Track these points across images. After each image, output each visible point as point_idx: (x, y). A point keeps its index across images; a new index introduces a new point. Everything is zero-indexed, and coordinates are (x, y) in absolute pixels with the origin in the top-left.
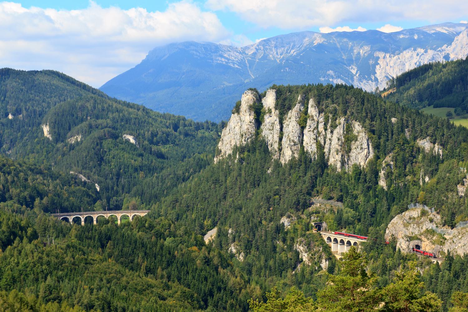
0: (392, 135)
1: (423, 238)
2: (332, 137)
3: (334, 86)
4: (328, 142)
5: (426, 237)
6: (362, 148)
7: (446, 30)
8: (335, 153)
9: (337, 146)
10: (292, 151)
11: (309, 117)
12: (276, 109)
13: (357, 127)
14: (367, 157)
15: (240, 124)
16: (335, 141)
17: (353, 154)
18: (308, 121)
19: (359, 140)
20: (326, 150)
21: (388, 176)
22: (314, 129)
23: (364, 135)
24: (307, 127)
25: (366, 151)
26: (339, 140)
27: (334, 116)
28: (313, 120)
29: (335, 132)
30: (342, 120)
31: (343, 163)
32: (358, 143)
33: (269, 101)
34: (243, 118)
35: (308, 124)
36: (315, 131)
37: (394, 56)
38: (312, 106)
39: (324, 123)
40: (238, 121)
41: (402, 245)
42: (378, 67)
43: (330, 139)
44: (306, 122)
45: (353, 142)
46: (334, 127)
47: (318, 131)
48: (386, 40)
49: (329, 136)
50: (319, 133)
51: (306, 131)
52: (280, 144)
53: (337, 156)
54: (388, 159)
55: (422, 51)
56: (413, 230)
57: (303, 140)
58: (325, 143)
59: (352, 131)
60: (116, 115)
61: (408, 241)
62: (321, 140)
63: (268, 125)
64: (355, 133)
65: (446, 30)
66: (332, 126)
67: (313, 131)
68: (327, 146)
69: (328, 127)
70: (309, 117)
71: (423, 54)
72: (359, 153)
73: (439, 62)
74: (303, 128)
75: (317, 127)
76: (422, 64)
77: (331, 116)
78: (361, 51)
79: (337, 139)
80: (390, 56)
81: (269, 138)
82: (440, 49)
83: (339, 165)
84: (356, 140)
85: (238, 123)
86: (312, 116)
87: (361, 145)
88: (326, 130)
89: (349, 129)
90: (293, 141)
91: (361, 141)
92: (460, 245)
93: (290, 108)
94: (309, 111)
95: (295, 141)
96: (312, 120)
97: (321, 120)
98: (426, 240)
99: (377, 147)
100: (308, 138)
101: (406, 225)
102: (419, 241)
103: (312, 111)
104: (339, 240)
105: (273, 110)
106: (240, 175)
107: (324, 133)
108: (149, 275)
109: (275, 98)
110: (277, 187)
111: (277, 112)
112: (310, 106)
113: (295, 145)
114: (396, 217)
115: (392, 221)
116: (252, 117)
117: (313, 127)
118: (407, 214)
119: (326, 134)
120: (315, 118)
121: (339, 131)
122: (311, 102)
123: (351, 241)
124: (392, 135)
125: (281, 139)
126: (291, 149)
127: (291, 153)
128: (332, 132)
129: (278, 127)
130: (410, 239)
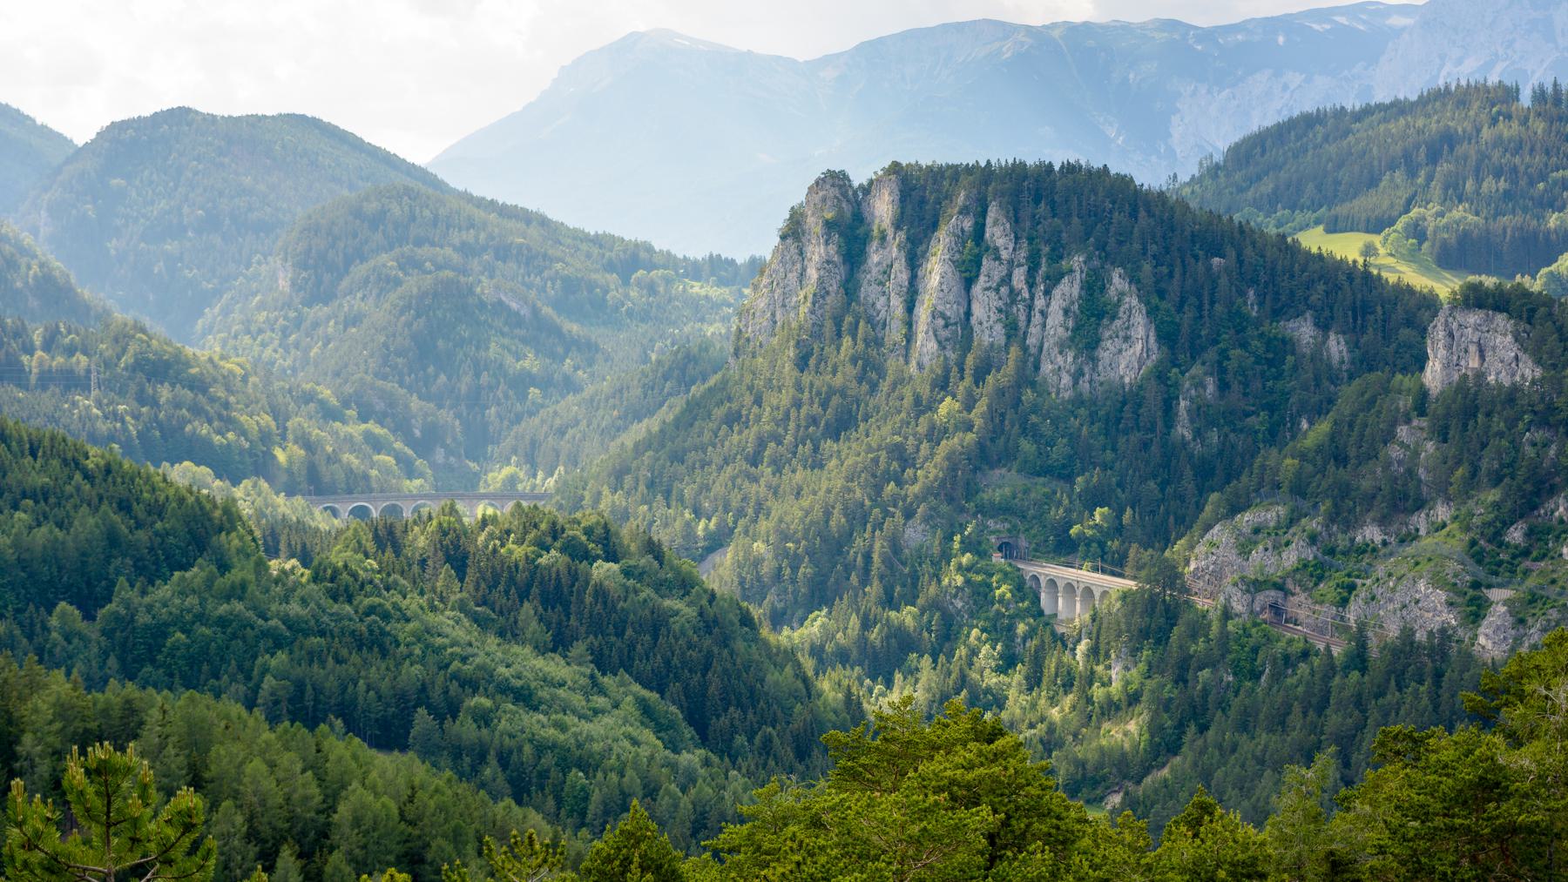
0: (1212, 303)
1: (1290, 585)
2: (1048, 305)
3: (1057, 168)
4: (1037, 319)
5: (1300, 583)
6: (1127, 339)
7: (1364, 22)
8: (1056, 350)
9: (1061, 330)
10: (939, 342)
11: (987, 249)
12: (897, 227)
13: (1117, 281)
14: (1141, 362)
15: (799, 266)
16: (1056, 317)
17: (1105, 354)
18: (985, 262)
19: (1121, 314)
20: (1031, 341)
21: (1200, 412)
22: (999, 285)
23: (1135, 302)
24: (982, 279)
25: (1139, 346)
26: (1066, 312)
27: (1053, 250)
28: (998, 258)
29: (1057, 292)
30: (1077, 261)
31: (1077, 375)
32: (1118, 323)
33: (883, 209)
34: (809, 249)
35: (983, 269)
36: (1004, 290)
37: (1219, 92)
38: (996, 223)
39: (1026, 267)
40: (796, 257)
41: (1234, 604)
42: (1175, 119)
43: (1042, 312)
44: (979, 265)
45: (1105, 321)
46: (1054, 280)
47: (1012, 290)
48: (1199, 47)
49: (1039, 303)
50: (1013, 293)
51: (977, 289)
52: (909, 324)
53: (1060, 359)
54: (1196, 370)
55: (1295, 79)
56: (1260, 560)
57: (968, 314)
58: (1029, 321)
59: (1103, 289)
60: (469, 236)
61: (1248, 591)
62: (1020, 311)
63: (875, 270)
64: (1112, 292)
65: (1364, 22)
66: (1048, 277)
67: (997, 290)
68: (1033, 330)
69: (1039, 279)
70: (987, 249)
71: (1300, 86)
72: (1120, 351)
73: (1343, 108)
74: (969, 283)
75: (1007, 280)
76: (1296, 113)
77: (1046, 249)
78: (1131, 76)
79: (1061, 312)
80: (1209, 92)
81: (878, 306)
82: (1346, 73)
83: (1066, 380)
84: (1114, 317)
85: (793, 264)
86: (997, 249)
87: (1128, 328)
88: (1031, 285)
89: (1094, 286)
90: (943, 316)
91: (1125, 317)
92: (1391, 607)
93: (934, 226)
94: (987, 235)
95: (948, 314)
96: (995, 259)
97: (1023, 254)
98: (1298, 589)
99: (1167, 336)
100: (984, 307)
101: (1244, 550)
102: (1280, 594)
103: (998, 233)
104: (1061, 585)
105: (890, 232)
106: (798, 404)
107: (1026, 295)
108: (162, 793)
109: (897, 198)
110: (898, 439)
111: (902, 235)
112: (989, 221)
113: (946, 326)
114: (1217, 527)
115: (1208, 536)
116: (832, 249)
117: (997, 278)
118: (1247, 519)
119: (1032, 298)
120: (1005, 255)
121: (1069, 290)
122: (993, 212)
123: (1093, 588)
124: (1212, 303)
125: (910, 307)
126: (936, 336)
127: (936, 346)
128: (1047, 293)
129: (904, 277)
130: (1255, 586)
